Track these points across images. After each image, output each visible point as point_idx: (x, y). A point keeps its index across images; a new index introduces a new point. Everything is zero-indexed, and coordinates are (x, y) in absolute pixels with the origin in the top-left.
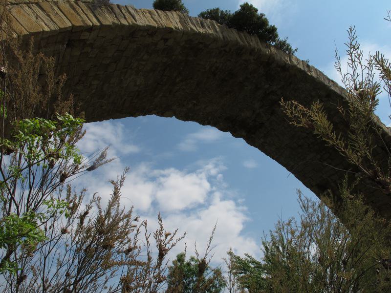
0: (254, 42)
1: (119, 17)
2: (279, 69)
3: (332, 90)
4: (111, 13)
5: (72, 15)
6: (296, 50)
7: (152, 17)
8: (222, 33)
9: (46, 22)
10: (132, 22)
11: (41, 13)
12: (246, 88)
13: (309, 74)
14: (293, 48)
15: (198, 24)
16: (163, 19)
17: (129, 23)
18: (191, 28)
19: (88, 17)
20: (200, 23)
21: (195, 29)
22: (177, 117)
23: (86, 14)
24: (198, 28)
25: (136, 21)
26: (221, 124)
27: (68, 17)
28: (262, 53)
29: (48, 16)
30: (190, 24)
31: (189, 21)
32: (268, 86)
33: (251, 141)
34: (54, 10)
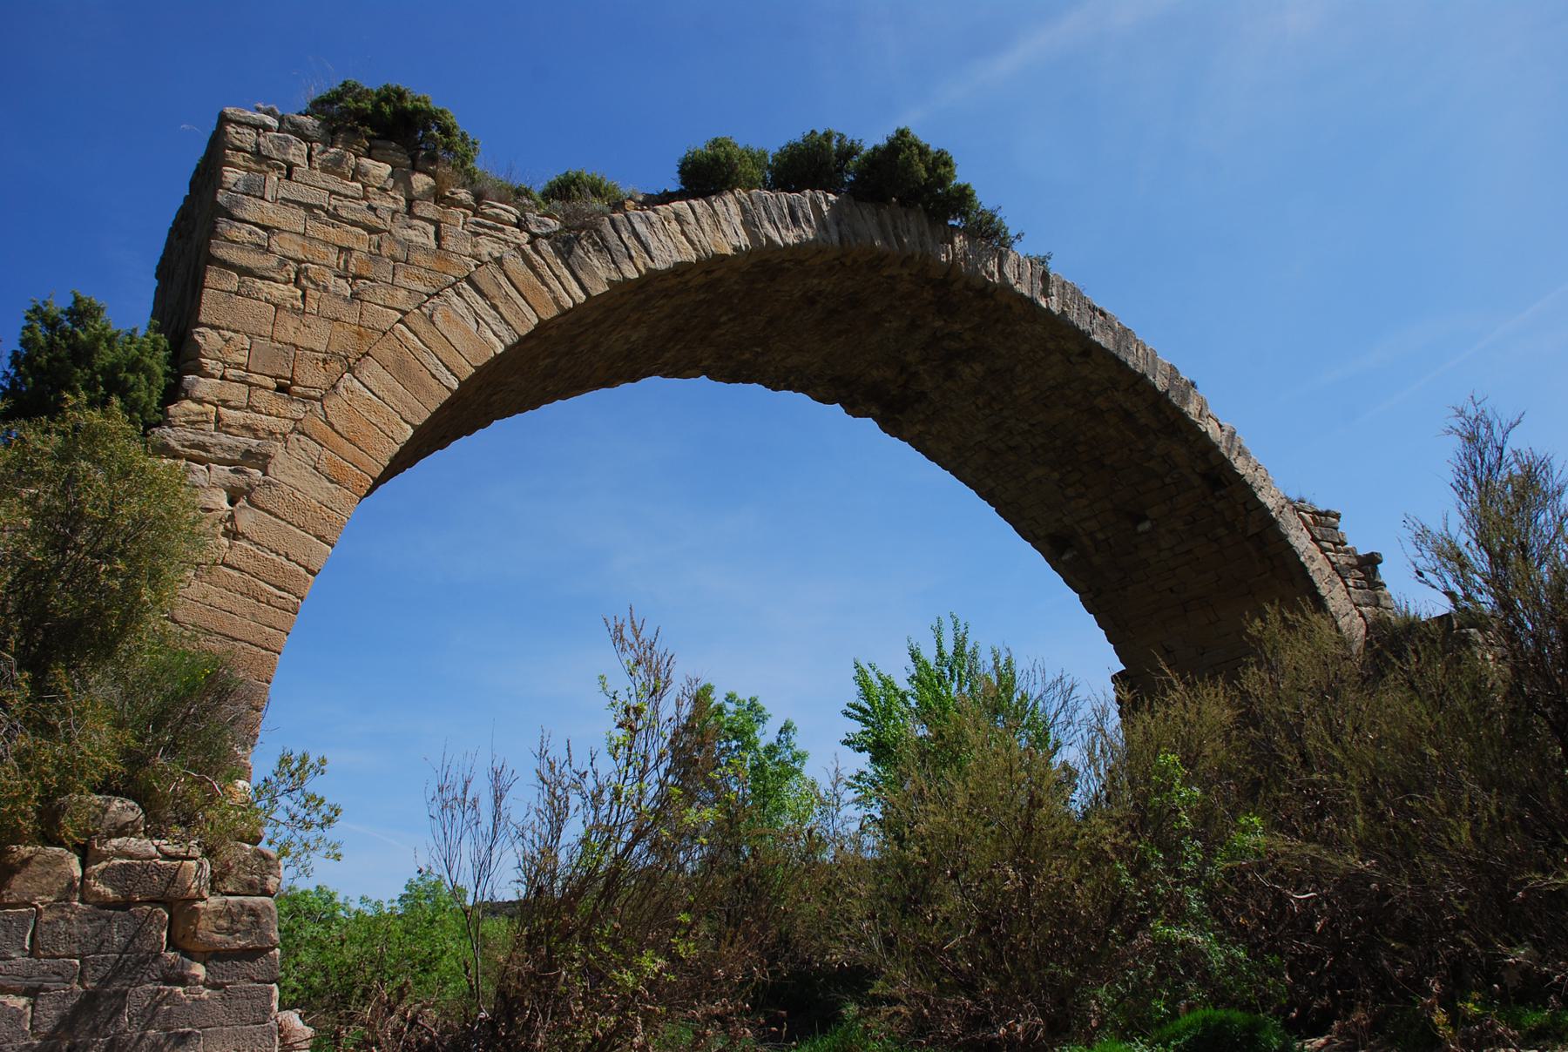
0: (912, 231)
1: (619, 259)
2: (971, 294)
3: (1093, 342)
4: (600, 251)
5: (534, 288)
6: (1018, 237)
7: (683, 233)
8: (838, 224)
9: (494, 327)
10: (645, 264)
11: (481, 305)
12: (887, 325)
13: (1043, 303)
14: (1012, 233)
15: (782, 217)
16: (706, 228)
17: (639, 271)
18: (768, 237)
19: (561, 283)
20: (786, 211)
21: (778, 239)
22: (712, 377)
23: (558, 277)
24: (783, 232)
25: (653, 261)
26: (819, 389)
27: (529, 300)
28: (930, 262)
29: (495, 307)
30: (766, 224)
31: (763, 213)
32: (942, 323)
33: (890, 425)
34: (499, 286)
